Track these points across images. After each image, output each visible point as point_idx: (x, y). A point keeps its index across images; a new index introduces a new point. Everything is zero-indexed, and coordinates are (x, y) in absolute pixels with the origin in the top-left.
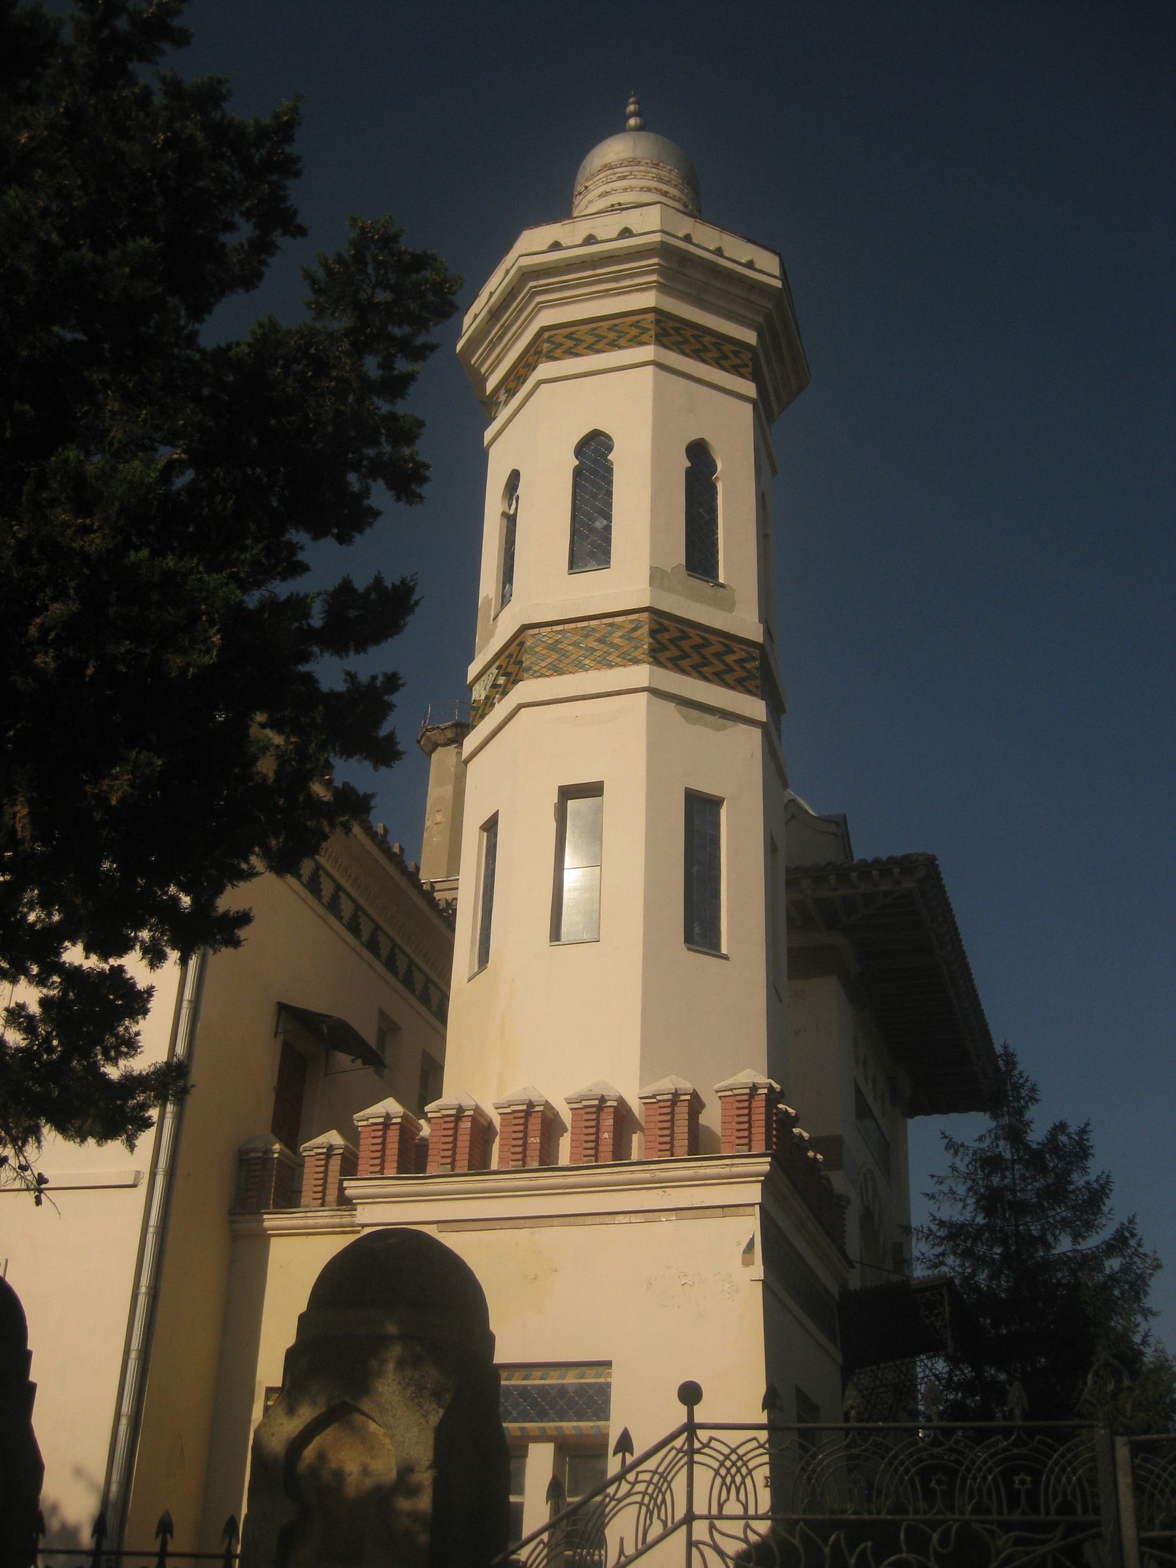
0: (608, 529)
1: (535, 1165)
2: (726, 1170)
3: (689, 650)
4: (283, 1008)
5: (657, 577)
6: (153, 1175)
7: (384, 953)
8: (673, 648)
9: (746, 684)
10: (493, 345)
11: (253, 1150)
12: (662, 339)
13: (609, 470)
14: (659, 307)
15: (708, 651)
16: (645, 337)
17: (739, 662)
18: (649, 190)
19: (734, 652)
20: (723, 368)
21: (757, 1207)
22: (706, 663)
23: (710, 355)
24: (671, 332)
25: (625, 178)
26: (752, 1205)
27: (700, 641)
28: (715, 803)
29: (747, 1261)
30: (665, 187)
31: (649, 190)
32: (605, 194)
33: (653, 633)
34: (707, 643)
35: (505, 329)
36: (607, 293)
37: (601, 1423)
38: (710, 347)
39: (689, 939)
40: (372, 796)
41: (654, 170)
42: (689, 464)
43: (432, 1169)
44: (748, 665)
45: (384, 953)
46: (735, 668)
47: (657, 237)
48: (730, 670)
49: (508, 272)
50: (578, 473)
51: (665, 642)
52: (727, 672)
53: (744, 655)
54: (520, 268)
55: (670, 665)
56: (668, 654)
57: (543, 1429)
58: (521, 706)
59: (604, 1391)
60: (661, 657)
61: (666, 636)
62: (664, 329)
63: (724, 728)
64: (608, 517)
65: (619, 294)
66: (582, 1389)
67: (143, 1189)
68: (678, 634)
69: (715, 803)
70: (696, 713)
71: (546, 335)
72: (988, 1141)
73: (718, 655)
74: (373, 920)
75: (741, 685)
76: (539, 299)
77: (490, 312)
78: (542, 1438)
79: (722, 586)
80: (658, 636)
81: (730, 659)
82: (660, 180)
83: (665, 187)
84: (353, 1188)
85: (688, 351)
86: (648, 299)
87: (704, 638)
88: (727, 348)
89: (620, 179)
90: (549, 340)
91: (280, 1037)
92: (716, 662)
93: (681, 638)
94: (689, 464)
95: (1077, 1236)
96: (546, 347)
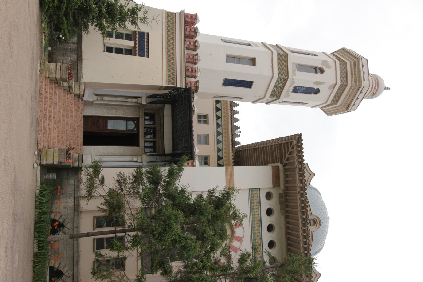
42: (315, 88)
54: (359, 58)
58: (272, 52)
59: (144, 56)
66: (144, 52)
78: (135, 44)
94: (315, 88)
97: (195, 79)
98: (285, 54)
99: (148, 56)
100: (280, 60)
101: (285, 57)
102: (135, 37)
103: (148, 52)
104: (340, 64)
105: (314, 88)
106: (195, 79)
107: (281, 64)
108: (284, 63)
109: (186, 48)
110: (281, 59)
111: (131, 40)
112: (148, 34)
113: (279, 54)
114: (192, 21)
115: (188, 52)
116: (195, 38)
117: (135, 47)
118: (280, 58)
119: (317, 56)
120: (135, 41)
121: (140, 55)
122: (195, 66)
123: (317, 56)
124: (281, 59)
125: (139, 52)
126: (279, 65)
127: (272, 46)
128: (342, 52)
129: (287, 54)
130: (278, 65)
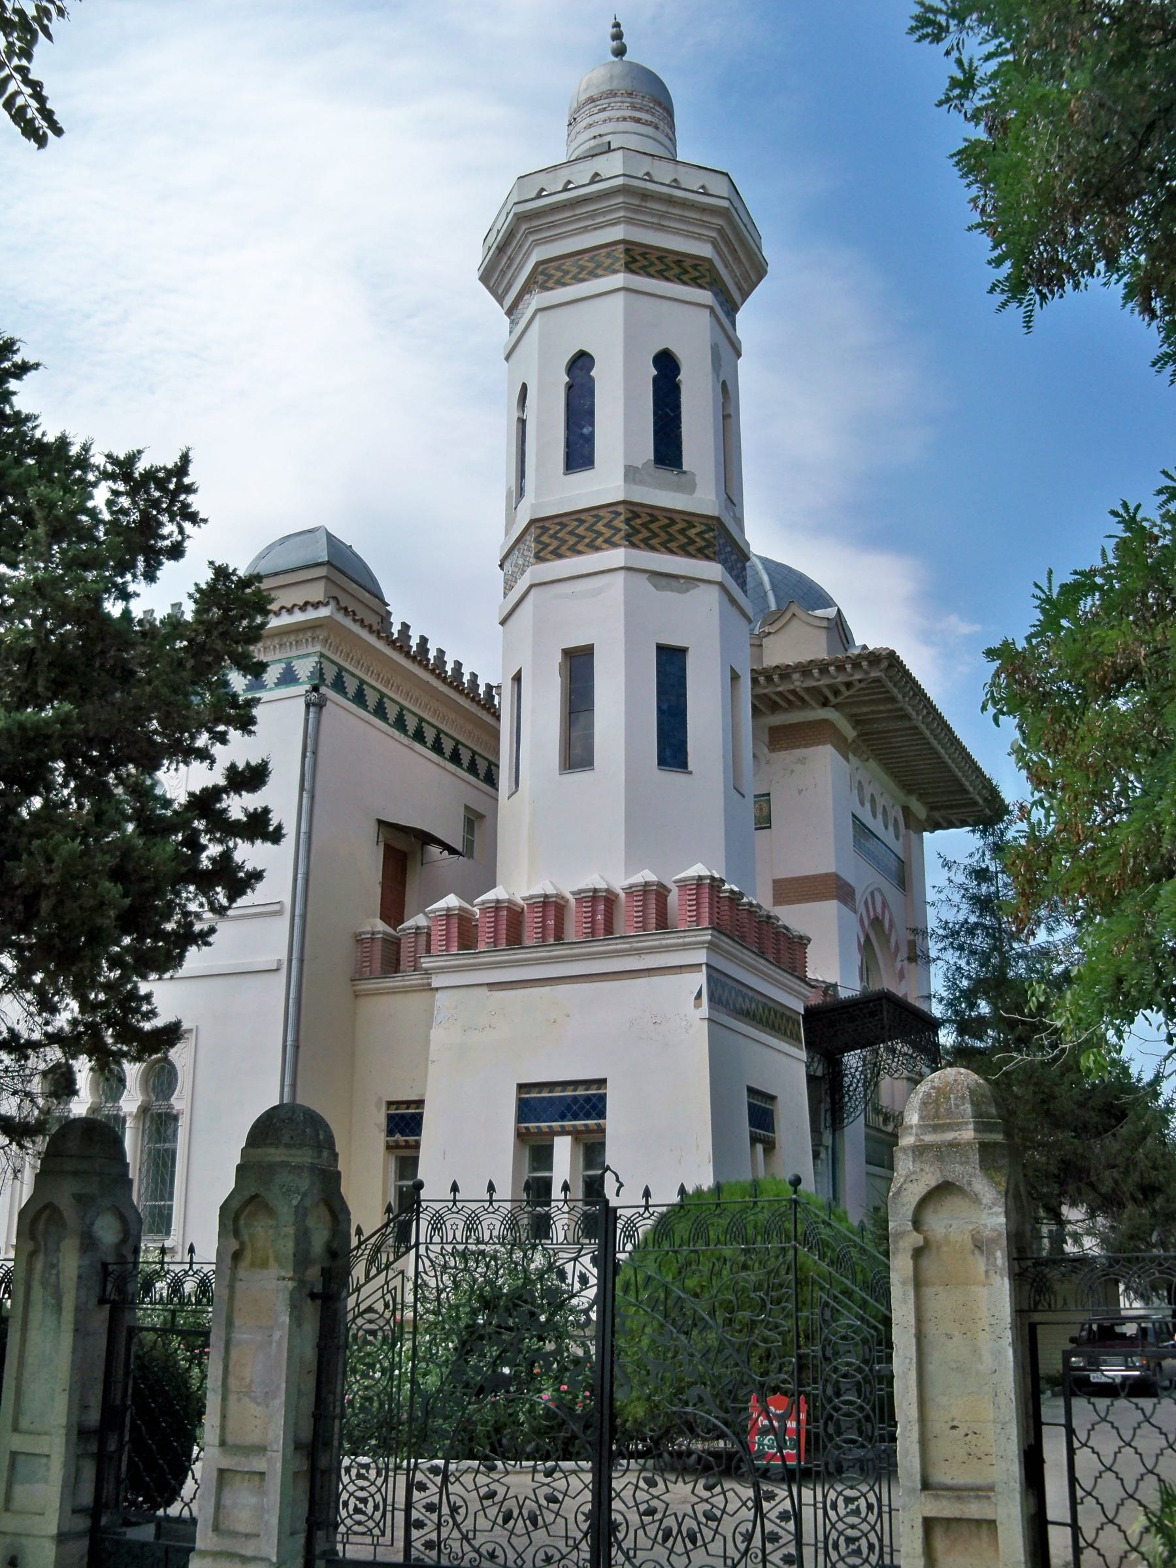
0: (593, 433)
1: (551, 941)
2: (681, 940)
3: (657, 530)
4: (381, 823)
5: (631, 474)
6: (290, 961)
7: (466, 761)
8: (644, 530)
9: (706, 552)
10: (503, 273)
11: (364, 933)
12: (631, 266)
13: (592, 380)
14: (628, 238)
15: (673, 530)
16: (617, 266)
17: (699, 534)
18: (625, 119)
19: (695, 527)
20: (685, 283)
21: (704, 968)
22: (672, 539)
23: (672, 272)
24: (638, 258)
25: (604, 109)
26: (701, 965)
27: (667, 521)
28: (682, 651)
29: (697, 1005)
30: (638, 114)
31: (625, 119)
32: (590, 126)
33: (627, 521)
34: (673, 522)
35: (511, 260)
36: (586, 229)
37: (601, 1121)
38: (672, 265)
39: (663, 762)
40: (263, 871)
41: (629, 100)
42: (656, 373)
43: (482, 947)
44: (706, 536)
45: (466, 761)
46: (697, 540)
47: (620, 181)
48: (692, 542)
49: (499, 231)
50: (570, 387)
51: (638, 527)
52: (688, 544)
53: (703, 528)
55: (642, 545)
56: (641, 536)
57: (562, 1127)
59: (602, 1098)
60: (634, 539)
61: (639, 521)
62: (632, 257)
63: (687, 590)
64: (592, 424)
65: (595, 229)
66: (588, 1099)
67: (284, 971)
68: (649, 518)
69: (682, 651)
70: (664, 581)
71: (541, 268)
72: (977, 857)
73: (682, 531)
74: (453, 739)
75: (703, 553)
76: (531, 238)
77: (497, 247)
78: (563, 1132)
79: (685, 472)
80: (632, 523)
81: (692, 532)
82: (633, 107)
83: (638, 114)
84: (427, 963)
85: (653, 273)
86: (617, 233)
87: (670, 519)
88: (687, 263)
89: (600, 111)
90: (542, 273)
91: (382, 845)
92: (680, 537)
93: (652, 522)
94: (656, 373)
95: (1050, 930)
96: (541, 278)
97: (669, 891)
98: (532, 529)
99: (602, 1082)
100: (558, 548)
101: (545, 530)
102: (540, 1132)
103: (587, 1083)
104: (544, 288)
105: (655, 379)
106: (669, 891)
107: (572, 540)
108: (569, 528)
109: (559, 937)
110: (555, 543)
111: (551, 1147)
112: (521, 1087)
113: (539, 558)
114: (455, 923)
115: (572, 931)
116: (515, 904)
117: (576, 1134)
118: (551, 548)
119: (524, 388)
120: (553, 1133)
121: (602, 1114)
122: (622, 895)
123: (524, 388)
124: (555, 543)
125: (588, 1116)
126: (580, 547)
127: (508, 587)
128: (498, 282)
129: (533, 522)
130: (580, 553)
